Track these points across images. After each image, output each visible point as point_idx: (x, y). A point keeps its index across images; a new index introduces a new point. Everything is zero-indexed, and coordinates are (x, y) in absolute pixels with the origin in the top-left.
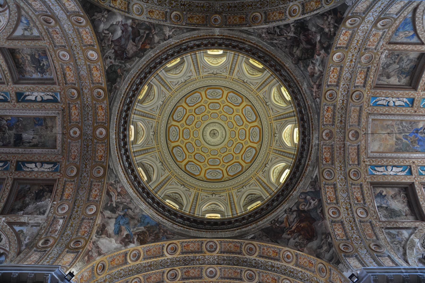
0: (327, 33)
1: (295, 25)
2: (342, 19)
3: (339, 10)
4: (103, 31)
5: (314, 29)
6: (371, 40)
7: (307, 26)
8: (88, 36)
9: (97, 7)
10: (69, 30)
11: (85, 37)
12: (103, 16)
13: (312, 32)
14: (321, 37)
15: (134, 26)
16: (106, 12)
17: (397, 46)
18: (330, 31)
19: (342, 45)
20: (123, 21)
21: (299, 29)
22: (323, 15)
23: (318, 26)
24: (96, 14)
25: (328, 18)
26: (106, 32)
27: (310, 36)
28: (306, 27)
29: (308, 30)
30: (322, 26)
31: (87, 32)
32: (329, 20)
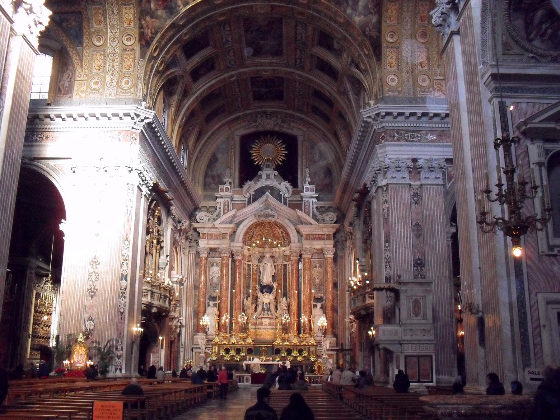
0: (146, 15)
1: (178, 8)
2: (140, 40)
3: (146, 48)
4: (375, 13)
5: (160, 12)
6: (100, 15)
7: (166, 12)
8: (390, 14)
9: (372, 45)
10: (407, 22)
11: (394, 11)
12: (370, 30)
13: (160, 9)
14: (151, 8)
15: (345, 4)
16: (367, 33)
17: (70, 10)
18: (145, 20)
19: (128, 7)
20: (354, 15)
21: (173, 5)
22: (156, 33)
23: (157, 18)
24: (375, 37)
25: (151, 33)
26: (372, 11)
27: (160, 3)
28: (167, 10)
29: (164, 9)
30: (153, 20)
31: (390, 18)
32: (149, 31)
